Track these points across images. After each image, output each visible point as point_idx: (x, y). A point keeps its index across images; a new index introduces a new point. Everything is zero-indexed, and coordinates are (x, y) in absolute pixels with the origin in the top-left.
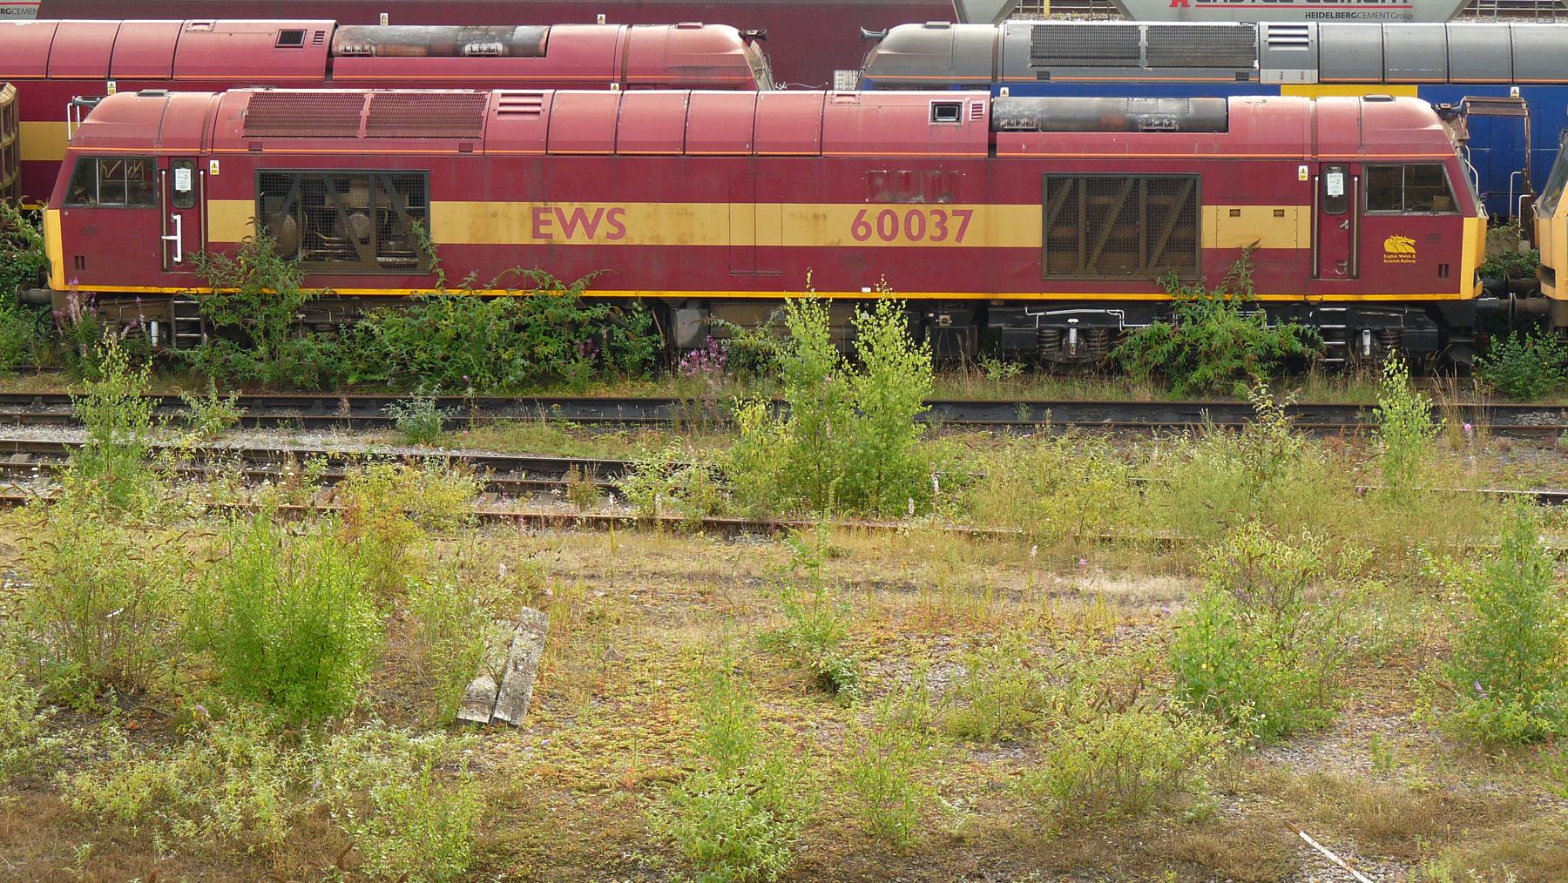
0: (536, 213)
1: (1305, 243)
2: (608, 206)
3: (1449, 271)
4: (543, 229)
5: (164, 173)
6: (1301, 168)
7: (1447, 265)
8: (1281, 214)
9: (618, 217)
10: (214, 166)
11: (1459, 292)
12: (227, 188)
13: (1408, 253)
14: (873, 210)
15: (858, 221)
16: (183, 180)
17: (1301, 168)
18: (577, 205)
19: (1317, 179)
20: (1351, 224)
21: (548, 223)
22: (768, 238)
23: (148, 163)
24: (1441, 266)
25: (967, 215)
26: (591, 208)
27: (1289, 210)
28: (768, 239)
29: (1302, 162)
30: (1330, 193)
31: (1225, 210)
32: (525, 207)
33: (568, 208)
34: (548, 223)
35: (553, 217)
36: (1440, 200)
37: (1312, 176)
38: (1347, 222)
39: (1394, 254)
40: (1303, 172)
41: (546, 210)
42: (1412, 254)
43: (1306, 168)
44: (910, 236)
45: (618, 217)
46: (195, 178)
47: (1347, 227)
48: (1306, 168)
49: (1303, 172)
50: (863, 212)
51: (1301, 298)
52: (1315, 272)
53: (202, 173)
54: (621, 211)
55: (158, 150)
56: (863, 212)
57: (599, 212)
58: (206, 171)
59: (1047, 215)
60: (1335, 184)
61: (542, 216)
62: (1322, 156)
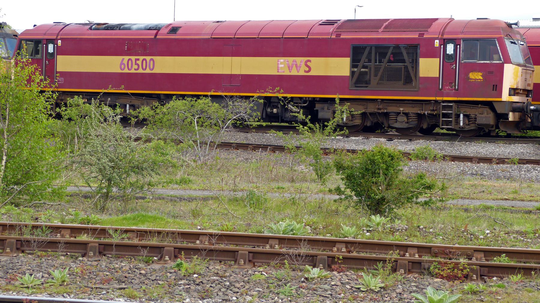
3: (497, 88)
5: (45, 45)
6: (436, 41)
7: (496, 85)
10: (59, 42)
11: (501, 97)
13: (479, 79)
17: (436, 41)
19: (442, 46)
20: (456, 67)
24: (494, 85)
29: (436, 39)
30: (448, 53)
36: (495, 56)
37: (440, 45)
38: (454, 65)
39: (473, 79)
40: (437, 43)
42: (481, 79)
43: (438, 41)
47: (454, 68)
48: (438, 41)
49: (437, 43)
51: (434, 98)
52: (441, 87)
53: (56, 45)
58: (57, 45)
60: (450, 49)
62: (445, 36)
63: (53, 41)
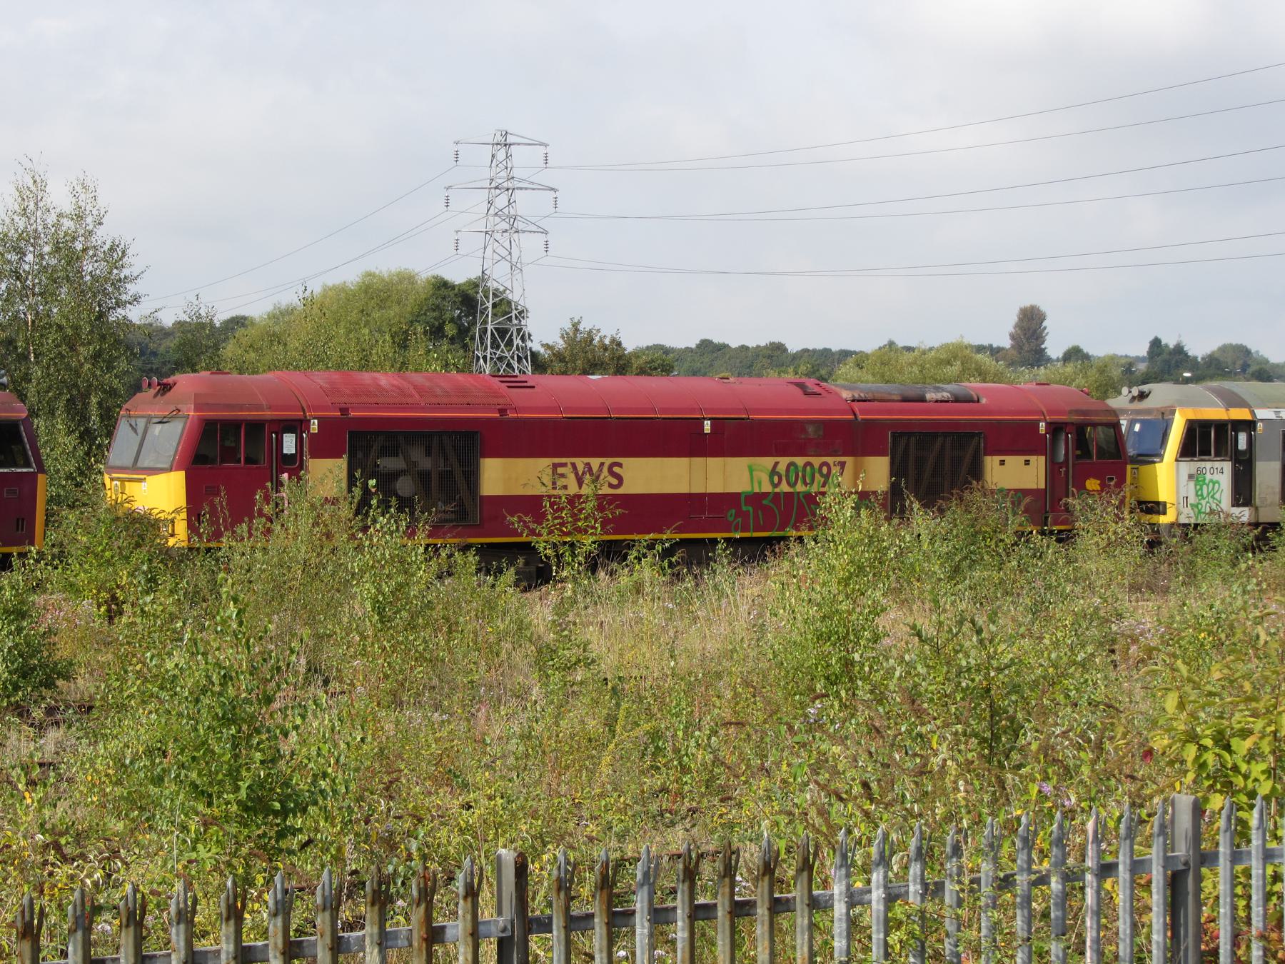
0: (555, 466)
1: (1042, 486)
2: (608, 461)
4: (561, 482)
8: (1027, 462)
9: (616, 469)
12: (323, 447)
14: (784, 462)
15: (774, 471)
16: (289, 444)
18: (586, 460)
21: (562, 476)
22: (715, 486)
23: (256, 427)
25: (843, 465)
26: (595, 462)
27: (1033, 459)
28: (715, 487)
31: (997, 459)
32: (545, 462)
33: (580, 462)
34: (562, 476)
35: (566, 470)
41: (564, 465)
44: (788, 483)
45: (616, 469)
46: (299, 443)
50: (776, 464)
54: (620, 465)
55: (268, 414)
56: (776, 464)
57: (602, 464)
59: (892, 463)
61: (560, 470)
63: (297, 426)
